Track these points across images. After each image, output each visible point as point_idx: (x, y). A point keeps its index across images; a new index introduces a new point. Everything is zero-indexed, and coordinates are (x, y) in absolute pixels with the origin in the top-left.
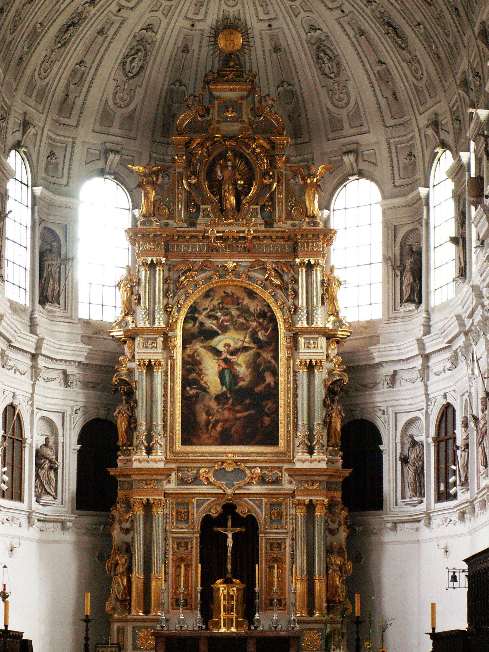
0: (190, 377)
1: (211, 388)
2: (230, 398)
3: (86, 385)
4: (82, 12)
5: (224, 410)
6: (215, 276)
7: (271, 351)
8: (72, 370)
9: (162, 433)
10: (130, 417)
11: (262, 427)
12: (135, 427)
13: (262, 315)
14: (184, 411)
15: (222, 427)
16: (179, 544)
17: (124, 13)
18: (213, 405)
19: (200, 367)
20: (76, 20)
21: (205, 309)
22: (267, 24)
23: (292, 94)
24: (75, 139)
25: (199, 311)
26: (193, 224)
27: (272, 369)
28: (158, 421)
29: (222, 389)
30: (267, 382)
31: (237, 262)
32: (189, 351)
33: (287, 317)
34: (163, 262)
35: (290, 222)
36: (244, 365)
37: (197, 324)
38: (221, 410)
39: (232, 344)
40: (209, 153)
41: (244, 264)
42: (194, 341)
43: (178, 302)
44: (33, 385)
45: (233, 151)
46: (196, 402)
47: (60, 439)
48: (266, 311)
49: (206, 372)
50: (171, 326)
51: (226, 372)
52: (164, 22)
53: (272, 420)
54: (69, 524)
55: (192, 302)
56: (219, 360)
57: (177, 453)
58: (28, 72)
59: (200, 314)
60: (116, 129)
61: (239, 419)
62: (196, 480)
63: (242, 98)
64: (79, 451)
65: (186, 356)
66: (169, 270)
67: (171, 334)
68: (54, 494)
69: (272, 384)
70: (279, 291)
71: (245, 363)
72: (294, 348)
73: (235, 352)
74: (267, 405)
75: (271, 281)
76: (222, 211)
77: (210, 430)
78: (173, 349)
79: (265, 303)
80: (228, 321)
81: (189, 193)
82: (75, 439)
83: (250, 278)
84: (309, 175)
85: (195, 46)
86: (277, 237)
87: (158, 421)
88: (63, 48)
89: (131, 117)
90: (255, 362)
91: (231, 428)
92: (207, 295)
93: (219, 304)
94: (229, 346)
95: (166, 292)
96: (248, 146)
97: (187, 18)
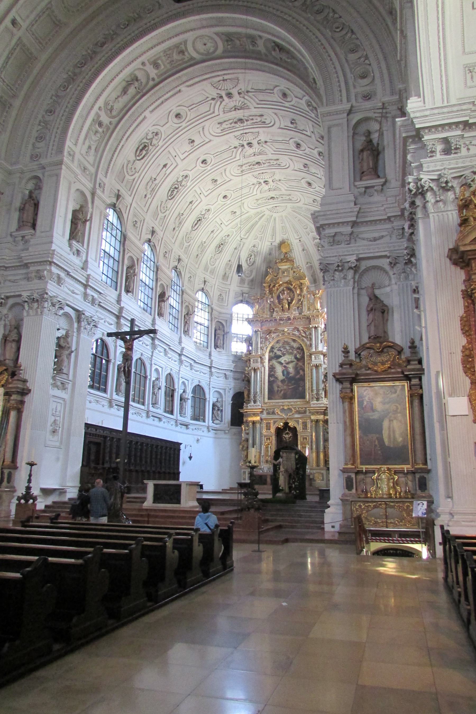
3: (235, 379)
4: (225, 240)
8: (228, 373)
13: (298, 348)
16: (267, 439)
17: (243, 240)
18: (280, 384)
20: (223, 243)
22: (298, 240)
23: (311, 266)
24: (229, 289)
26: (272, 316)
28: (258, 390)
32: (271, 364)
35: (308, 312)
39: (287, 360)
40: (277, 289)
44: (210, 378)
45: (286, 287)
47: (224, 399)
50: (264, 355)
51: (285, 371)
52: (260, 243)
54: (227, 432)
57: (266, 403)
58: (204, 261)
60: (246, 285)
62: (273, 413)
63: (289, 268)
64: (232, 403)
68: (220, 419)
70: (304, 339)
73: (288, 363)
75: (302, 335)
76: (283, 310)
81: (270, 305)
82: (230, 399)
83: (293, 334)
84: (316, 294)
85: (274, 252)
86: (303, 318)
87: (258, 390)
88: (219, 254)
89: (252, 281)
92: (277, 342)
95: (261, 343)
96: (292, 285)
97: (268, 241)
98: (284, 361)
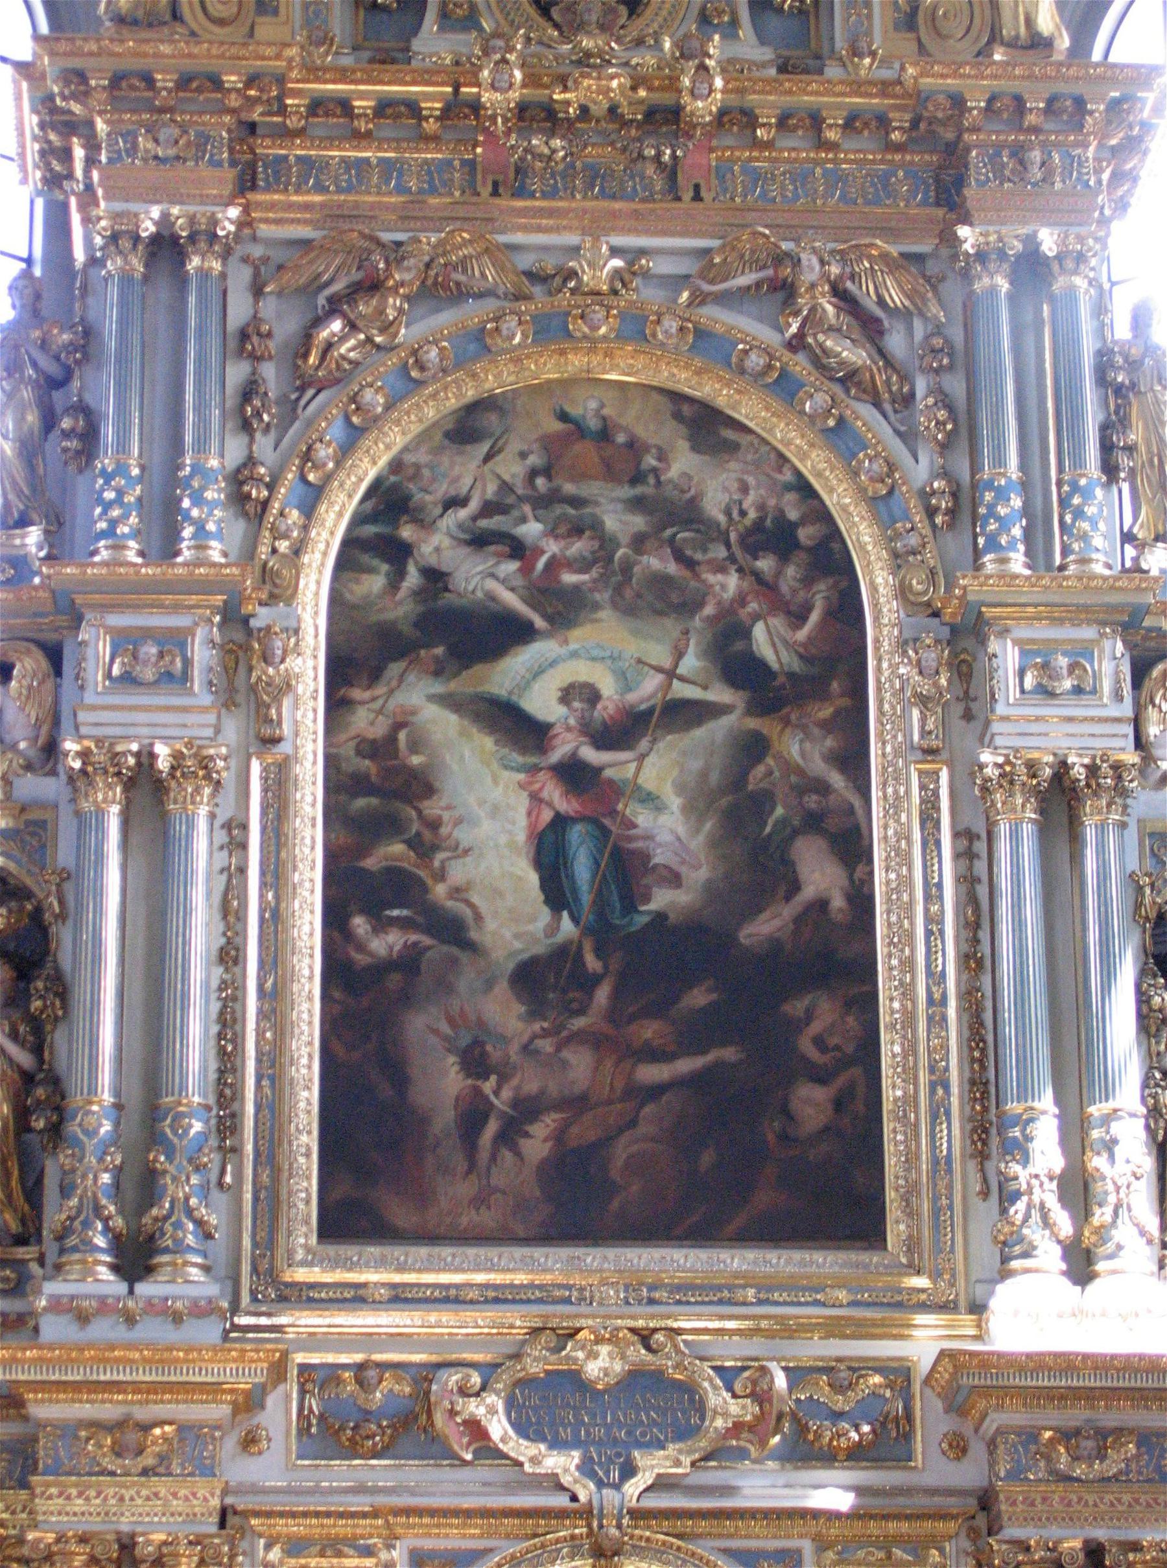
0: (371, 863)
1: (491, 925)
2: (594, 981)
5: (568, 1040)
6: (511, 322)
7: (827, 726)
9: (211, 1159)
10: (28, 1079)
11: (784, 1137)
12: (56, 1131)
14: (339, 1050)
15: (559, 1136)
19: (432, 808)
21: (454, 502)
25: (421, 508)
27: (833, 824)
29: (553, 929)
30: (809, 892)
31: (634, 255)
33: (913, 540)
34: (227, 228)
36: (675, 802)
37: (413, 578)
38: (546, 1046)
39: (608, 687)
41: (661, 266)
42: (395, 669)
43: (307, 456)
46: (406, 999)
48: (793, 515)
49: (463, 836)
51: (576, 834)
53: (839, 1105)
55: (383, 461)
56: (534, 770)
59: (425, 524)
61: (656, 1091)
65: (348, 750)
66: (257, 291)
67: (262, 617)
69: (838, 902)
70: (866, 411)
71: (680, 789)
72: (958, 709)
74: (809, 1016)
77: (484, 1155)
78: (277, 700)
79: (788, 476)
80: (583, 565)
83: (701, 334)
86: (851, 124)
90: (737, 782)
91: (606, 1141)
93: (533, 473)
94: (592, 695)
98: (567, 695)
